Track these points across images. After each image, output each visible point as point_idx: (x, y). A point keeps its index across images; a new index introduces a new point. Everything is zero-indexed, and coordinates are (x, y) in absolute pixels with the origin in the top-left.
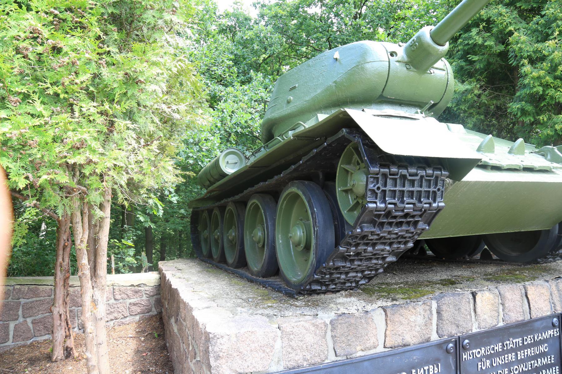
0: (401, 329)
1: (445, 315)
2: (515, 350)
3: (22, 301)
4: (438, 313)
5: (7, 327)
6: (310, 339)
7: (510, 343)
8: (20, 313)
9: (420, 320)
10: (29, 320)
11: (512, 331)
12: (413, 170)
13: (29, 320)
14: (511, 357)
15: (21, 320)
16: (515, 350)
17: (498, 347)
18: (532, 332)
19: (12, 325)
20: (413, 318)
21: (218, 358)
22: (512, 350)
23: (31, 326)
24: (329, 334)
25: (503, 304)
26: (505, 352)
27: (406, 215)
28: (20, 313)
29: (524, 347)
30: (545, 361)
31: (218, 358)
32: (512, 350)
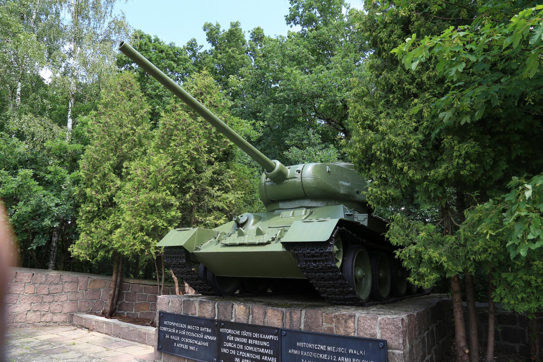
2: (248, 338)
4: (218, 308)
7: (245, 333)
14: (245, 340)
16: (248, 338)
17: (238, 333)
18: (259, 332)
22: (245, 337)
24: (182, 305)
26: (240, 336)
30: (267, 351)
32: (245, 337)
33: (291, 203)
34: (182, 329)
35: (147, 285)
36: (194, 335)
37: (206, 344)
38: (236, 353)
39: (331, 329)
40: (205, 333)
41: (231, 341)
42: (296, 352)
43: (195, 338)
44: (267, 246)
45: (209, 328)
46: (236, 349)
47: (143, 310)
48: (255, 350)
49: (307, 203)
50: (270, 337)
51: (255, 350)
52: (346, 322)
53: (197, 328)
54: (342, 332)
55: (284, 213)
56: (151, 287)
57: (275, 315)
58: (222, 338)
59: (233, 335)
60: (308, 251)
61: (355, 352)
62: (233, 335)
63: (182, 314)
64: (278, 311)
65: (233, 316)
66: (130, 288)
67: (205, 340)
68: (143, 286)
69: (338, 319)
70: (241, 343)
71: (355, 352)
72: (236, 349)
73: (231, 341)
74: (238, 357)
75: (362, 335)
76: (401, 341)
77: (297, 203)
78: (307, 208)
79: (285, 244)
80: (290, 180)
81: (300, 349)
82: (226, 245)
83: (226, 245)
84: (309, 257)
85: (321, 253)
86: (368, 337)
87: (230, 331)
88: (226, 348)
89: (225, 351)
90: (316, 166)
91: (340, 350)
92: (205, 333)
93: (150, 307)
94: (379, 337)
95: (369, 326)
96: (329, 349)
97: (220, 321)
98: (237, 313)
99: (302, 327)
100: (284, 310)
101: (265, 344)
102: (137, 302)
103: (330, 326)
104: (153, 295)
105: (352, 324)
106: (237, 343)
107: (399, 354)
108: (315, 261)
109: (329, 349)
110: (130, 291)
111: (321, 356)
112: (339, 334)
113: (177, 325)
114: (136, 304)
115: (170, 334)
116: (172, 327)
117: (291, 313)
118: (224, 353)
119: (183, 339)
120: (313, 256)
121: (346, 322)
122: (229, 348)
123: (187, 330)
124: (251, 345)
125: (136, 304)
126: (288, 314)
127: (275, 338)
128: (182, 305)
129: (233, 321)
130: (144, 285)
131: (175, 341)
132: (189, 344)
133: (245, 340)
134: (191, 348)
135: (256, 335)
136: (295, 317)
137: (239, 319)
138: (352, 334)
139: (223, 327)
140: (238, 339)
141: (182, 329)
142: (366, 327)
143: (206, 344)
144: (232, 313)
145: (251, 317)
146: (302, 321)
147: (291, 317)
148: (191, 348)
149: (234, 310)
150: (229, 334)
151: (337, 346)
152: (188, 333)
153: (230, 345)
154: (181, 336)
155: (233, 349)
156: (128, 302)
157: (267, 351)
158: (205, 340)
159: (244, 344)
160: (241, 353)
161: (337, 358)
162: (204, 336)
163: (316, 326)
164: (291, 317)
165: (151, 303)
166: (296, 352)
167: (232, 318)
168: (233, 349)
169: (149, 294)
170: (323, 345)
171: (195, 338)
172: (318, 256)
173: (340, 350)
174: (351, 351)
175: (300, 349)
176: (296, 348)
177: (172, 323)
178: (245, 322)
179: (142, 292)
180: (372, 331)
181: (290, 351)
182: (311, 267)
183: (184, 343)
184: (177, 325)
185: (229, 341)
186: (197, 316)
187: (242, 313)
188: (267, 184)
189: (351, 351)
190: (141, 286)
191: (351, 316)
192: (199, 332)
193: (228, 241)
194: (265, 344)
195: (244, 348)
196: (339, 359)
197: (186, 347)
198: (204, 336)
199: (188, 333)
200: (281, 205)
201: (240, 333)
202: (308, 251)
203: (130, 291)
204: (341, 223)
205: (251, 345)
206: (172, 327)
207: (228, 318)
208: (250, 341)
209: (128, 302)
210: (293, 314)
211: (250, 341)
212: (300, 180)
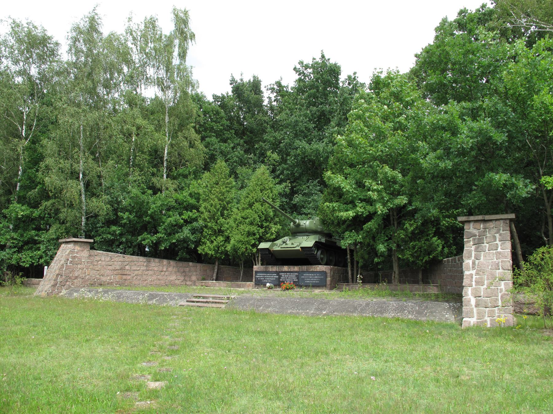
7: (288, 274)
34: (265, 276)
40: (274, 276)
49: (307, 234)
54: (316, 271)
55: (300, 238)
58: (280, 277)
67: (274, 278)
77: (304, 234)
78: (307, 236)
79: (301, 248)
90: (310, 222)
92: (274, 276)
97: (279, 272)
115: (260, 278)
116: (261, 275)
123: (267, 275)
136: (303, 268)
141: (265, 276)
151: (314, 274)
154: (265, 278)
158: (274, 278)
159: (287, 277)
192: (272, 276)
193: (282, 246)
200: (298, 234)
204: (316, 242)
206: (261, 275)
207: (282, 270)
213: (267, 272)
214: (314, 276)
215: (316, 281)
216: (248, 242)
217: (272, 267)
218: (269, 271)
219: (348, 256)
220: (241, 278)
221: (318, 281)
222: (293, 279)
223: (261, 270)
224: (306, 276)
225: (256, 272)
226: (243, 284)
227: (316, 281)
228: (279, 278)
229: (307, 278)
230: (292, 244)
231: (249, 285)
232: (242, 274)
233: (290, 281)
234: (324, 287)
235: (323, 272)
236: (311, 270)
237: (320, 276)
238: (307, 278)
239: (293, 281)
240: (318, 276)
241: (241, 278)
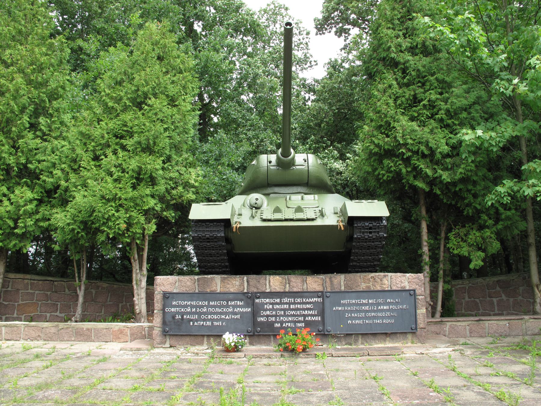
0: (228, 286)
1: (251, 283)
2: (289, 304)
3: (125, 294)
4: (248, 282)
5: (118, 305)
6: (188, 283)
7: (286, 300)
8: (124, 299)
9: (237, 283)
10: (128, 304)
11: (287, 294)
12: (207, 224)
13: (128, 304)
14: (286, 306)
15: (124, 303)
17: (278, 300)
18: (302, 297)
19: (120, 305)
20: (234, 282)
21: (157, 285)
22: (286, 303)
23: (128, 306)
24: (196, 283)
25: (289, 284)
26: (281, 303)
27: (208, 238)
28: (124, 299)
29: (295, 303)
30: (310, 312)
31: (157, 285)
32: (286, 303)
33: (289, 188)
34: (202, 307)
35: (34, 280)
36: (220, 310)
37: (238, 316)
38: (276, 319)
39: (369, 287)
41: (270, 310)
42: (340, 309)
43: (221, 313)
44: (315, 221)
45: (241, 300)
46: (276, 316)
47: (29, 313)
48: (298, 313)
50: (313, 300)
51: (298, 313)
52: (381, 280)
53: (225, 303)
54: (379, 288)
56: (41, 282)
57: (315, 282)
59: (271, 304)
60: (367, 224)
61: (392, 301)
62: (271, 304)
63: (197, 291)
64: (318, 278)
65: (268, 287)
66: (10, 284)
67: (236, 314)
68: (29, 281)
69: (375, 279)
70: (281, 310)
71: (392, 301)
72: (276, 316)
73: (270, 310)
74: (278, 322)
75: (394, 288)
76: (423, 289)
80: (297, 167)
81: (344, 305)
82: (265, 220)
83: (265, 220)
84: (367, 229)
85: (378, 226)
86: (399, 289)
87: (268, 300)
88: (262, 316)
89: (262, 319)
91: (380, 301)
93: (38, 309)
94: (407, 288)
95: (399, 282)
96: (370, 301)
98: (271, 284)
99: (343, 288)
100: (322, 276)
101: (309, 306)
102: (20, 302)
103: (367, 285)
104: (42, 292)
105: (387, 282)
106: (277, 309)
107: (422, 299)
108: (370, 233)
109: (370, 301)
110: (9, 289)
111: (363, 308)
112: (376, 289)
113: (194, 303)
114: (19, 305)
115: (182, 314)
116: (186, 306)
117: (330, 278)
118: (262, 323)
119: (203, 317)
120: (371, 228)
121: (381, 280)
122: (267, 316)
123: (208, 306)
124: (293, 310)
125: (19, 305)
126: (328, 280)
127: (320, 300)
128: (196, 283)
129: (268, 291)
130: (31, 280)
131: (192, 320)
132: (212, 320)
133: (286, 306)
134: (216, 323)
135: (299, 300)
137: (275, 289)
138: (387, 289)
139: (258, 298)
140: (277, 307)
141: (202, 307)
142: (398, 282)
143: (238, 316)
144: (266, 285)
145: (288, 285)
146: (342, 284)
147: (331, 282)
148: (216, 323)
149: (267, 281)
150: (266, 304)
151: (377, 299)
152: (211, 309)
153: (268, 312)
154: (200, 314)
155: (272, 316)
156: (6, 303)
157: (310, 312)
158: (236, 314)
159: (284, 310)
160: (281, 318)
161: (377, 308)
162: (233, 310)
163: (356, 287)
164: (331, 282)
165: (40, 303)
166: (340, 309)
167: (266, 289)
168: (272, 316)
169: (37, 292)
170: (365, 299)
171: (221, 313)
172: (375, 229)
173: (380, 301)
174: (389, 300)
175: (344, 305)
176: (340, 305)
177: (186, 302)
178: (282, 291)
179: (28, 290)
180: (402, 285)
181: (334, 309)
182: (366, 237)
183: (204, 320)
184: (194, 303)
185: (266, 310)
186: (218, 291)
187: (277, 284)
188: (272, 168)
189: (389, 300)
190: (26, 281)
191: (385, 276)
192: (227, 306)
194: (309, 306)
195: (285, 313)
196: (379, 308)
197: (209, 323)
198: (233, 310)
199: (211, 309)
201: (281, 301)
202: (367, 224)
203: (9, 289)
205: (293, 310)
208: (292, 307)
209: (6, 303)
210: (333, 279)
211: (292, 307)
212: (307, 168)
213: (203, 295)
214: (378, 304)
215: (382, 318)
216: (136, 203)
217: (223, 280)
218: (213, 293)
219: (425, 249)
220: (79, 310)
221: (388, 318)
222: (305, 316)
223: (183, 290)
224: (349, 305)
225: (167, 296)
226: (97, 330)
227: (382, 318)
228: (255, 314)
229: (351, 312)
230: (277, 210)
231: (121, 331)
232: (81, 299)
233: (295, 322)
234: (409, 336)
235: (404, 291)
236: (363, 286)
237: (397, 303)
238: (351, 312)
239: (305, 321)
240: (389, 304)
241: (79, 310)
